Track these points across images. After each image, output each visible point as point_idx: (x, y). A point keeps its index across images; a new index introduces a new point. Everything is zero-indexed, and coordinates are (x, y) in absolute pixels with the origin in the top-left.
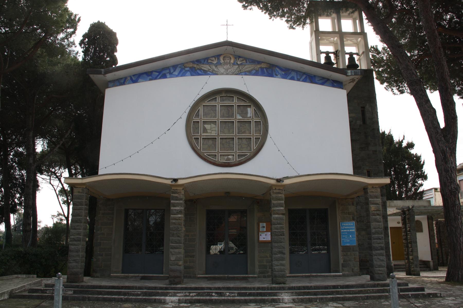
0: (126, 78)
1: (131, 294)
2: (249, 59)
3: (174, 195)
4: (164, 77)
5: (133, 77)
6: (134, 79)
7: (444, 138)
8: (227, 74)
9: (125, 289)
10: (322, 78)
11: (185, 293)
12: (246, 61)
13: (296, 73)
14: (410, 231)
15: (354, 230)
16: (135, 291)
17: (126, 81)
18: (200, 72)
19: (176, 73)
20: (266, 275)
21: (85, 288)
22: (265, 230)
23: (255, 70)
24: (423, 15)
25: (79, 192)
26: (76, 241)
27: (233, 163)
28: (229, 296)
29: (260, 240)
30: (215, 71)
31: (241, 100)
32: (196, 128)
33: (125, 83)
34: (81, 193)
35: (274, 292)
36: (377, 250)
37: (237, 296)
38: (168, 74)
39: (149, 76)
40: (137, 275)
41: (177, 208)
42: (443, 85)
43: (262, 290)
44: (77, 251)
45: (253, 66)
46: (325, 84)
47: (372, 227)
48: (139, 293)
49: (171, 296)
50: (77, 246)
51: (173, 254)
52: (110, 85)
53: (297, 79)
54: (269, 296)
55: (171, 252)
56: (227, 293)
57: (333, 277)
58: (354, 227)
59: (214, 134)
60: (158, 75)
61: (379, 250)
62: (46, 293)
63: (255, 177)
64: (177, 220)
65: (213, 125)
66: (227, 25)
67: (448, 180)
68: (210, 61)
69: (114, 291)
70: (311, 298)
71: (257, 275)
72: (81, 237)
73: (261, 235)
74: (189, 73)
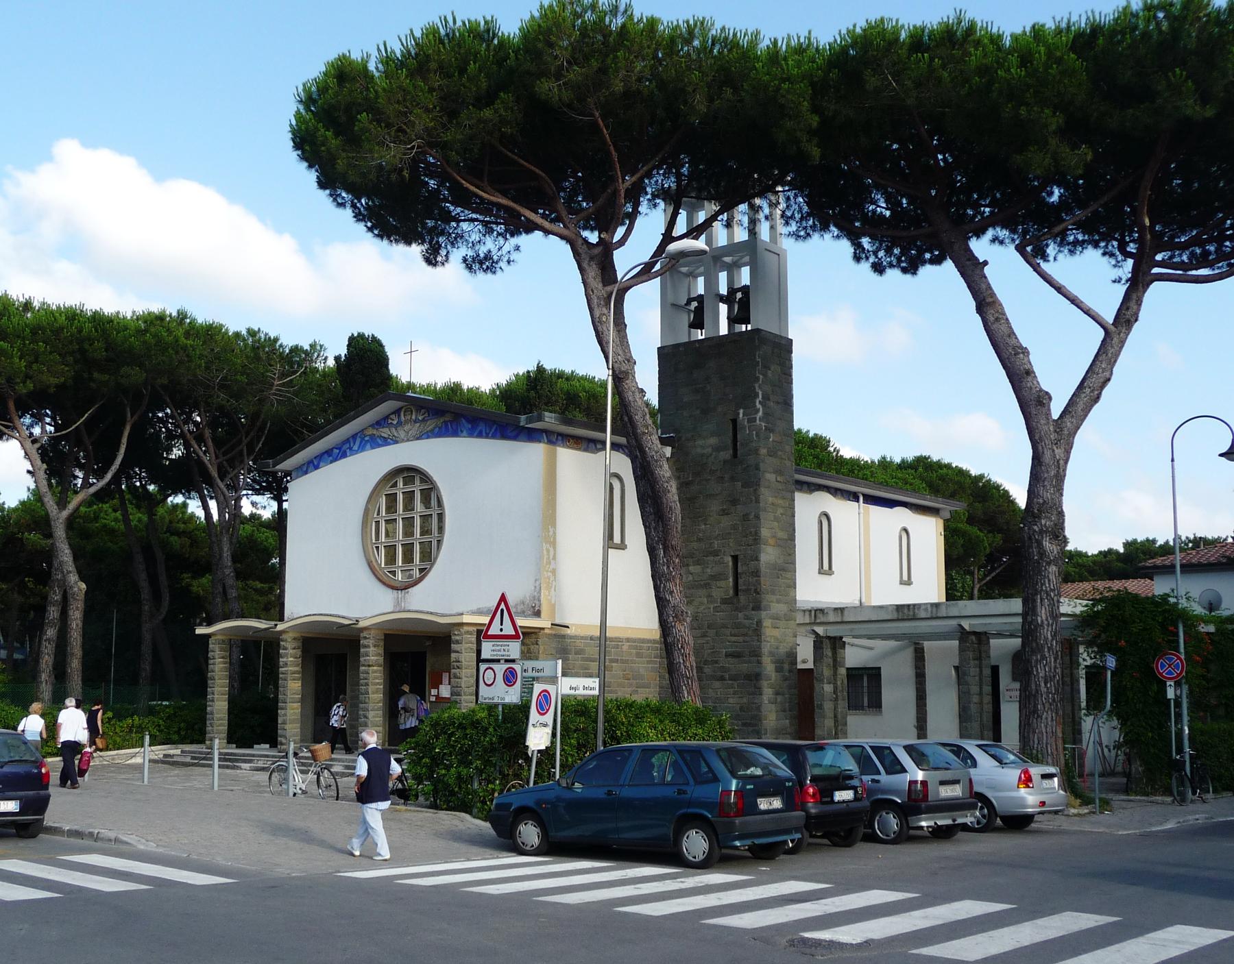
8: (408, 440)
19: (355, 448)
74: (368, 446)
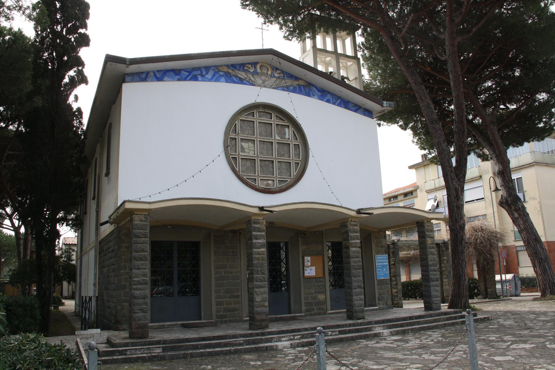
0: (148, 73)
1: (232, 344)
2: (286, 73)
3: (255, 225)
4: (195, 78)
5: (156, 73)
6: (158, 76)
7: (456, 177)
9: (217, 340)
10: (354, 105)
11: (290, 336)
12: (284, 75)
13: (331, 96)
14: (394, 265)
15: (387, 264)
16: (237, 341)
17: (149, 76)
18: (235, 80)
19: (209, 76)
20: (313, 313)
21: (168, 344)
22: (309, 264)
23: (292, 87)
24: (452, 60)
25: (141, 221)
26: (141, 284)
27: (274, 190)
28: (331, 335)
29: (306, 275)
30: (252, 81)
31: (279, 119)
32: (233, 146)
33: (147, 79)
34: (144, 221)
35: (369, 327)
36: (433, 281)
37: (339, 335)
38: (200, 76)
39: (177, 74)
40: (175, 323)
41: (260, 241)
42: (461, 128)
43: (353, 326)
44: (144, 297)
45: (290, 81)
46: (358, 112)
47: (429, 259)
48: (241, 342)
49: (276, 342)
50: (143, 291)
51: (258, 295)
52: (127, 79)
53: (333, 102)
54: (365, 331)
55: (256, 292)
56: (329, 332)
57: (371, 311)
58: (386, 260)
59: (251, 153)
60: (188, 76)
61: (435, 281)
62: (126, 354)
63: (344, 209)
64: (261, 254)
65: (251, 144)
66: (262, 29)
67: (458, 216)
68: (246, 68)
69: (212, 343)
70: (405, 329)
71: (304, 314)
72: (148, 279)
73: (306, 270)
